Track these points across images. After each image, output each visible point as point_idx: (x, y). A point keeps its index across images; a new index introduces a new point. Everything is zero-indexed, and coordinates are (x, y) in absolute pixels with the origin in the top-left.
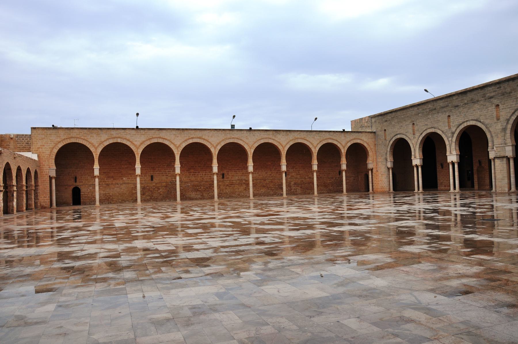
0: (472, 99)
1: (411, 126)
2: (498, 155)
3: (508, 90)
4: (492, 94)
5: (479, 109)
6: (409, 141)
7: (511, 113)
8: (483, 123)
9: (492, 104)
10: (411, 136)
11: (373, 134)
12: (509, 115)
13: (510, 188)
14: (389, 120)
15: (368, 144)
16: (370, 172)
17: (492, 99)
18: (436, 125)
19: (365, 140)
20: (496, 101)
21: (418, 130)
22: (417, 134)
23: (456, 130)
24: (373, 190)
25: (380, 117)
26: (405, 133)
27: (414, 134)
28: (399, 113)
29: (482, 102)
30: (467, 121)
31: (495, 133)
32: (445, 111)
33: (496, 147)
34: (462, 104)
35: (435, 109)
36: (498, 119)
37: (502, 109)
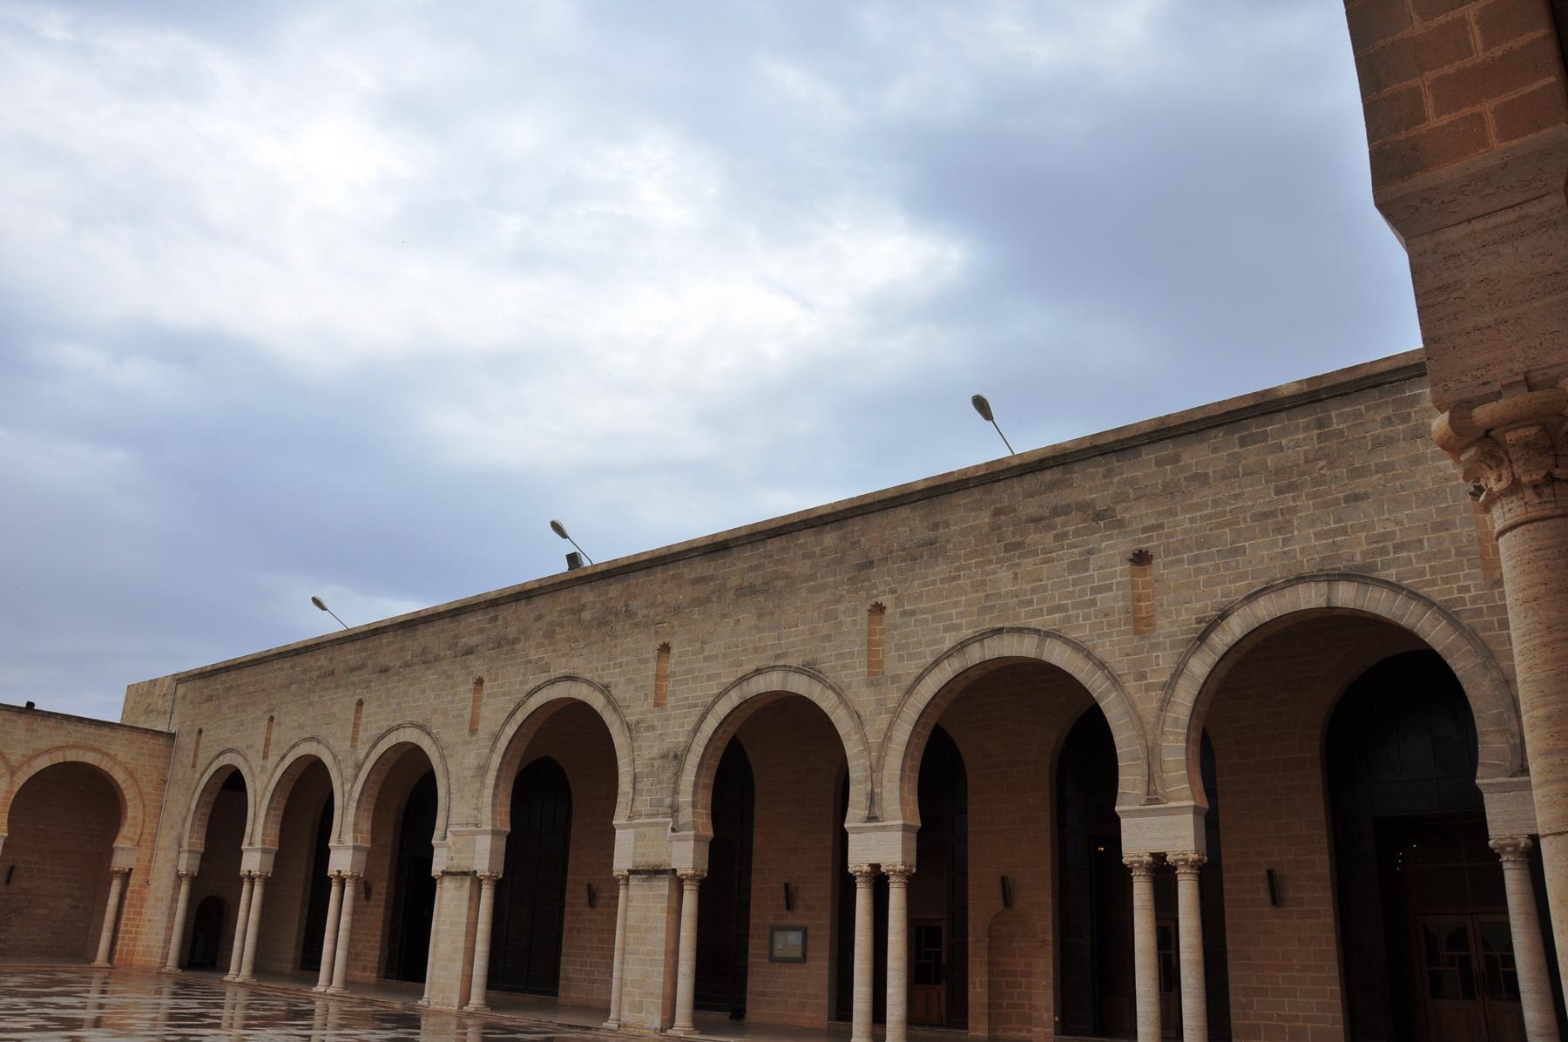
0: (424, 651)
4: (474, 640)
8: (435, 740)
9: (469, 674)
10: (256, 760)
11: (162, 741)
13: (466, 999)
15: (131, 774)
17: (470, 657)
19: (122, 763)
20: (478, 666)
25: (199, 683)
27: (265, 757)
30: (399, 727)
31: (458, 780)
32: (353, 684)
33: (455, 834)
34: (398, 664)
36: (473, 730)
37: (489, 695)
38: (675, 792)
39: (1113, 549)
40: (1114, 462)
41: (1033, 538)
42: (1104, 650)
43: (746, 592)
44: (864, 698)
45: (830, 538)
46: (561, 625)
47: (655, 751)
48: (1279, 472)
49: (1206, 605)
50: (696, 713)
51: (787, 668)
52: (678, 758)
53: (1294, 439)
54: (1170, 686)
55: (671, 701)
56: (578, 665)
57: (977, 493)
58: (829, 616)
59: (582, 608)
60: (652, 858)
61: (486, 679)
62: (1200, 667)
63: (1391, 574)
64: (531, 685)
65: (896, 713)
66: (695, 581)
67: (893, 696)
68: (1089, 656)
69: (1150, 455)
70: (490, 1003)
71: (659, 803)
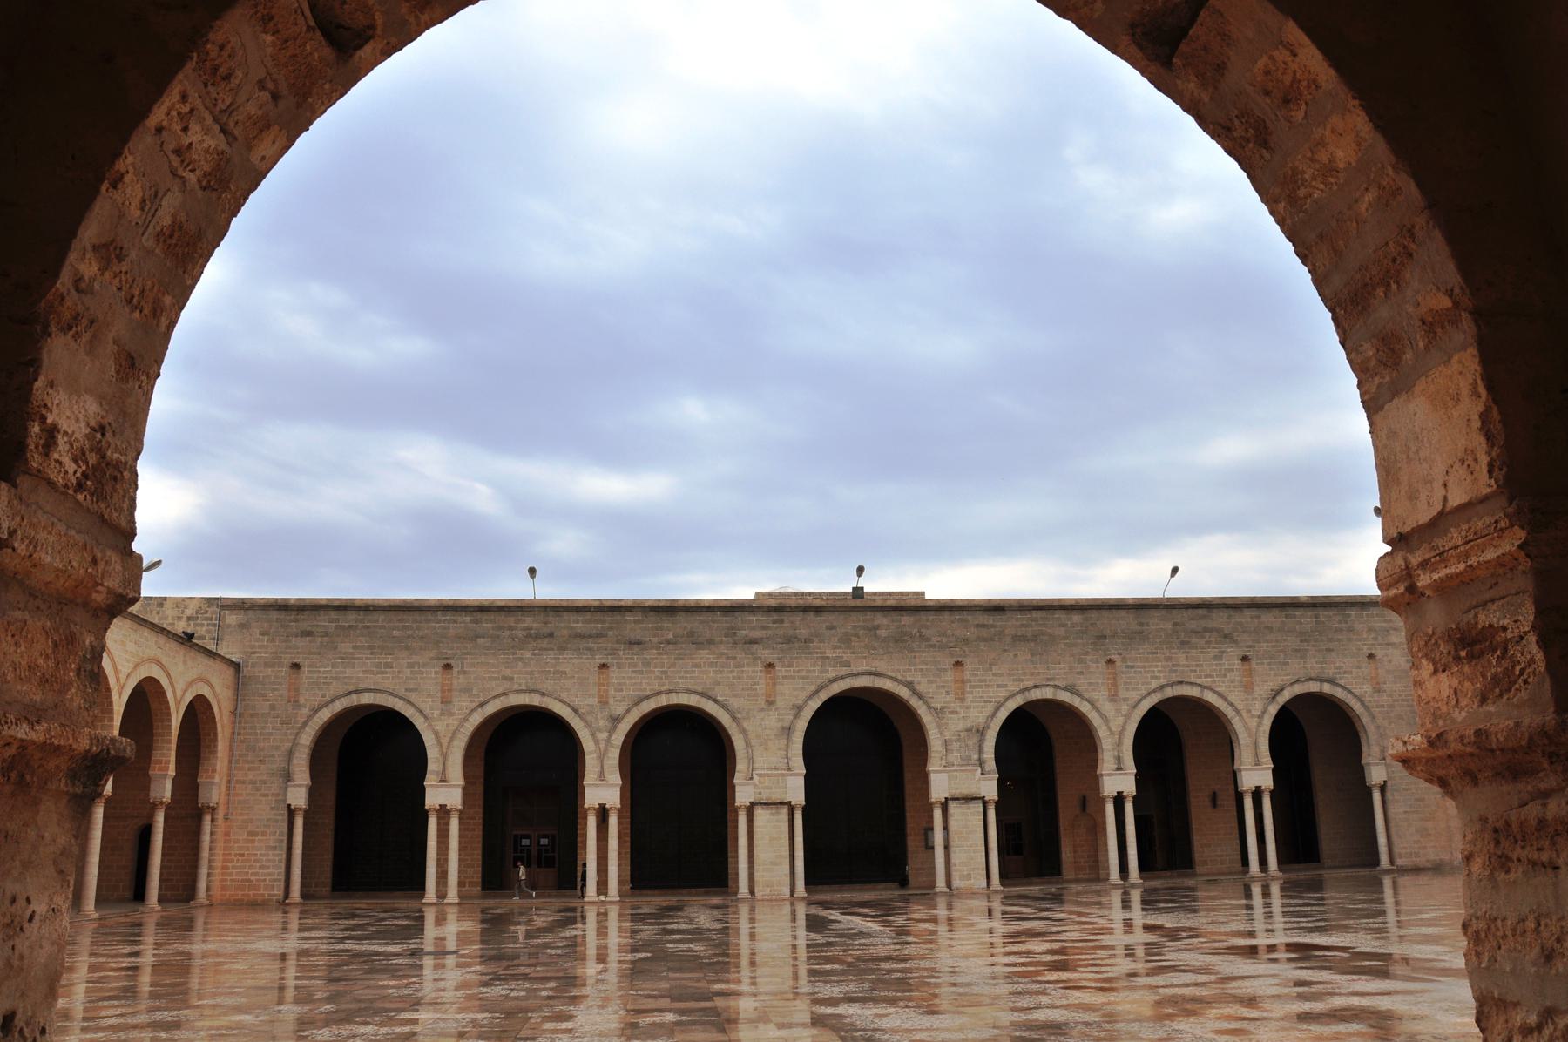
0: (691, 634)
1: (434, 671)
2: (764, 797)
3: (803, 632)
4: (757, 634)
5: (711, 665)
6: (419, 723)
7: (809, 693)
8: (724, 706)
12: (803, 696)
14: (326, 634)
16: (207, 819)
18: (548, 686)
20: (767, 654)
21: (467, 690)
22: (461, 704)
23: (628, 711)
24: (209, 896)
25: (274, 615)
26: (402, 692)
27: (446, 701)
28: (380, 618)
29: (723, 649)
30: (670, 691)
32: (589, 649)
34: (655, 640)
35: (551, 635)
36: (770, 703)
38: (980, 751)
39: (1234, 653)
40: (1231, 612)
41: (1194, 640)
42: (1232, 698)
43: (1017, 639)
44: (1108, 708)
45: (1076, 618)
46: (856, 635)
47: (961, 726)
48: (1301, 633)
49: (1273, 683)
50: (990, 708)
51: (1056, 687)
52: (981, 732)
53: (1306, 620)
54: (1260, 717)
55: (969, 697)
56: (881, 666)
57: (1163, 612)
58: (1080, 661)
59: (878, 627)
60: (965, 790)
61: (776, 662)
62: (1273, 710)
63: (1342, 682)
64: (832, 675)
65: (1127, 716)
66: (977, 626)
67: (1125, 708)
68: (1225, 699)
69: (1248, 613)
70: (807, 890)
71: (969, 758)
